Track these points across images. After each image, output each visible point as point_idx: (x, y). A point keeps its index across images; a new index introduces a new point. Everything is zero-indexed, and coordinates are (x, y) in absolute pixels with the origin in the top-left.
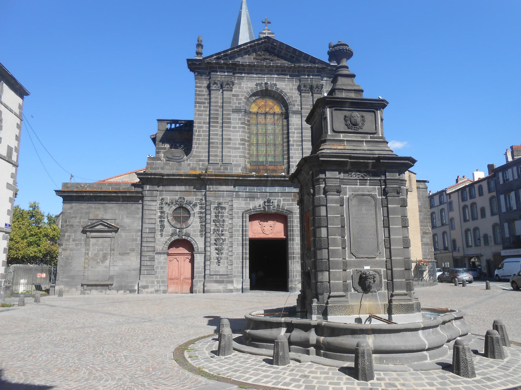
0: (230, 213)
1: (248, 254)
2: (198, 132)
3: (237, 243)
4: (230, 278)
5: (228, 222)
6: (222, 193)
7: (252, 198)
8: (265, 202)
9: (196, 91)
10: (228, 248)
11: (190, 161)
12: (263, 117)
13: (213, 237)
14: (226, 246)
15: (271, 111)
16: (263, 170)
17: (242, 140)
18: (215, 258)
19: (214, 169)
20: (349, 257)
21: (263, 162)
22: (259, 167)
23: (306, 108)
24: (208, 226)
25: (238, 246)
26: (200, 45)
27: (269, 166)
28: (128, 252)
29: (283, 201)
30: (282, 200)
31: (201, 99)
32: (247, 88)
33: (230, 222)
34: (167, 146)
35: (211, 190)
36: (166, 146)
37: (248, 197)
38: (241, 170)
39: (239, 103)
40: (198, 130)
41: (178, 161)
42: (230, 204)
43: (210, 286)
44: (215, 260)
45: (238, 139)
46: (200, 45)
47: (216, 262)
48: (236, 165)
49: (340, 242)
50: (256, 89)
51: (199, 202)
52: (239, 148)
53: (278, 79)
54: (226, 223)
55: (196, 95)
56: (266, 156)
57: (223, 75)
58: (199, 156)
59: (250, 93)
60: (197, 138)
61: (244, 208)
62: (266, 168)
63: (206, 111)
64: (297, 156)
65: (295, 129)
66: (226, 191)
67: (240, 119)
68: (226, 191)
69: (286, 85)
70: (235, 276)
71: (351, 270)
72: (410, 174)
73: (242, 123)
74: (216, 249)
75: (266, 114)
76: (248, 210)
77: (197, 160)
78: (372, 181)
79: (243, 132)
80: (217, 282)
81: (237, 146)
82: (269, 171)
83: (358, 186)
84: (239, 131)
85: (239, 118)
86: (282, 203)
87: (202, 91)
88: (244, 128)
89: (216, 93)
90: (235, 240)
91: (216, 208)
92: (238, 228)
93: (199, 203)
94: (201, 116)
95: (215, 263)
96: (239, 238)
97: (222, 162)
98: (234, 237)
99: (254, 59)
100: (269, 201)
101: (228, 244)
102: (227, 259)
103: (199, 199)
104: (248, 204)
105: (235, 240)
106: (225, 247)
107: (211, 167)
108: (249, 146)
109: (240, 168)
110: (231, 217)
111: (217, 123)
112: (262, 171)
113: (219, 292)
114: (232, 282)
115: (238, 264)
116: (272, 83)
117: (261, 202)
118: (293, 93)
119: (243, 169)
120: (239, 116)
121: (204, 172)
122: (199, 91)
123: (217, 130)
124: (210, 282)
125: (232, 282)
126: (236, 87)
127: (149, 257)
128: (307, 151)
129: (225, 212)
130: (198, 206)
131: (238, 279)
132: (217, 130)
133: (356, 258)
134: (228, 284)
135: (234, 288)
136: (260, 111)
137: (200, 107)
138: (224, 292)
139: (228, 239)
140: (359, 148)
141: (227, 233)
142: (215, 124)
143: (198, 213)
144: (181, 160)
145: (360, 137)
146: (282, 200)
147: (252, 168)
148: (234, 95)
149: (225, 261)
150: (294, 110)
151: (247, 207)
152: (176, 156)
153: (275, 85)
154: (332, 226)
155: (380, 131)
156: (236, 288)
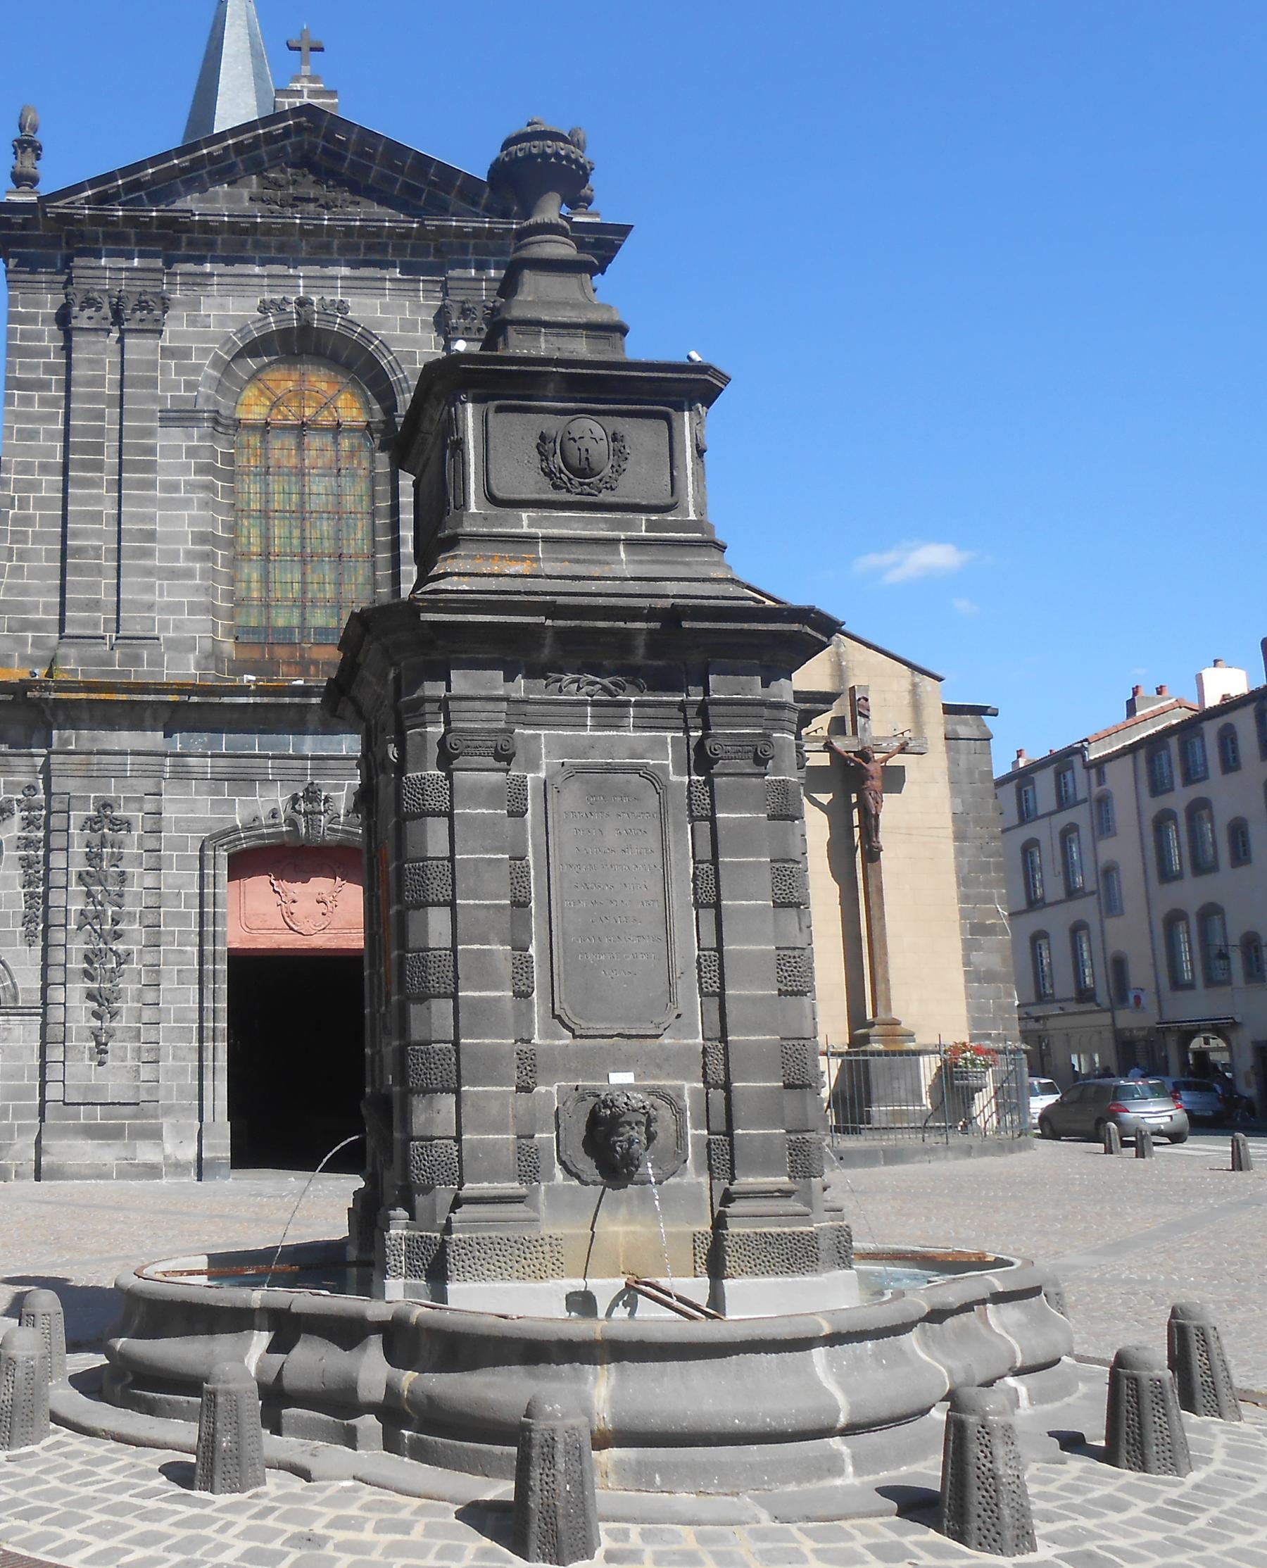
0: (151, 843)
1: (224, 1016)
3: (179, 971)
4: (146, 1117)
5: (139, 881)
6: (118, 759)
7: (243, 781)
8: (295, 799)
9: (11, 334)
10: (140, 991)
12: (290, 441)
13: (78, 946)
14: (132, 982)
15: (326, 419)
16: (289, 664)
17: (201, 538)
18: (87, 1033)
19: (82, 661)
20: (546, 1034)
21: (289, 630)
24: (56, 898)
26: (27, 145)
27: (315, 649)
31: (34, 368)
32: (222, 321)
33: (149, 881)
35: (72, 747)
37: (223, 776)
38: (198, 667)
39: (190, 386)
42: (149, 807)
43: (61, 1150)
44: (87, 1041)
45: (186, 533)
46: (27, 145)
47: (90, 1048)
49: (506, 969)
51: (21, 796)
52: (189, 574)
54: (133, 888)
55: (12, 350)
56: (303, 604)
57: (121, 269)
58: (22, 608)
61: (209, 824)
62: (302, 656)
63: (51, 418)
66: (133, 753)
68: (133, 753)
70: (168, 1110)
71: (554, 1089)
73: (201, 470)
74: (90, 996)
75: (302, 429)
76: (225, 834)
77: (15, 625)
78: (649, 711)
79: (205, 505)
80: (92, 1132)
81: (182, 564)
83: (589, 733)
84: (191, 499)
85: (188, 448)
87: (38, 336)
88: (209, 488)
89: (94, 343)
90: (172, 957)
91: (91, 824)
92: (182, 909)
93: (19, 801)
94: (31, 439)
95: (87, 1055)
96: (188, 948)
97: (118, 632)
98: (166, 944)
100: (311, 794)
102: (138, 1037)
103: (19, 783)
104: (224, 808)
105: (172, 957)
106: (128, 986)
107: (73, 652)
108: (233, 562)
109: (192, 658)
110: (152, 863)
111: (98, 466)
112: (283, 669)
113: (99, 1176)
114: (155, 1134)
115: (184, 1059)
117: (280, 799)
119: (203, 662)
120: (190, 437)
121: (40, 673)
122: (25, 335)
123: (98, 499)
124: (64, 1132)
125: (155, 1134)
126: (180, 318)
129: (127, 841)
130: (18, 815)
131: (182, 1121)
132: (98, 499)
133: (575, 1037)
134: (139, 1143)
135: (166, 1158)
136: (277, 418)
137: (27, 401)
138: (122, 1175)
139: (140, 952)
140: (596, 571)
141: (136, 926)
143: (15, 843)
145: (602, 526)
149: (126, 1047)
154: (472, 902)
155: (690, 499)
156: (173, 1160)
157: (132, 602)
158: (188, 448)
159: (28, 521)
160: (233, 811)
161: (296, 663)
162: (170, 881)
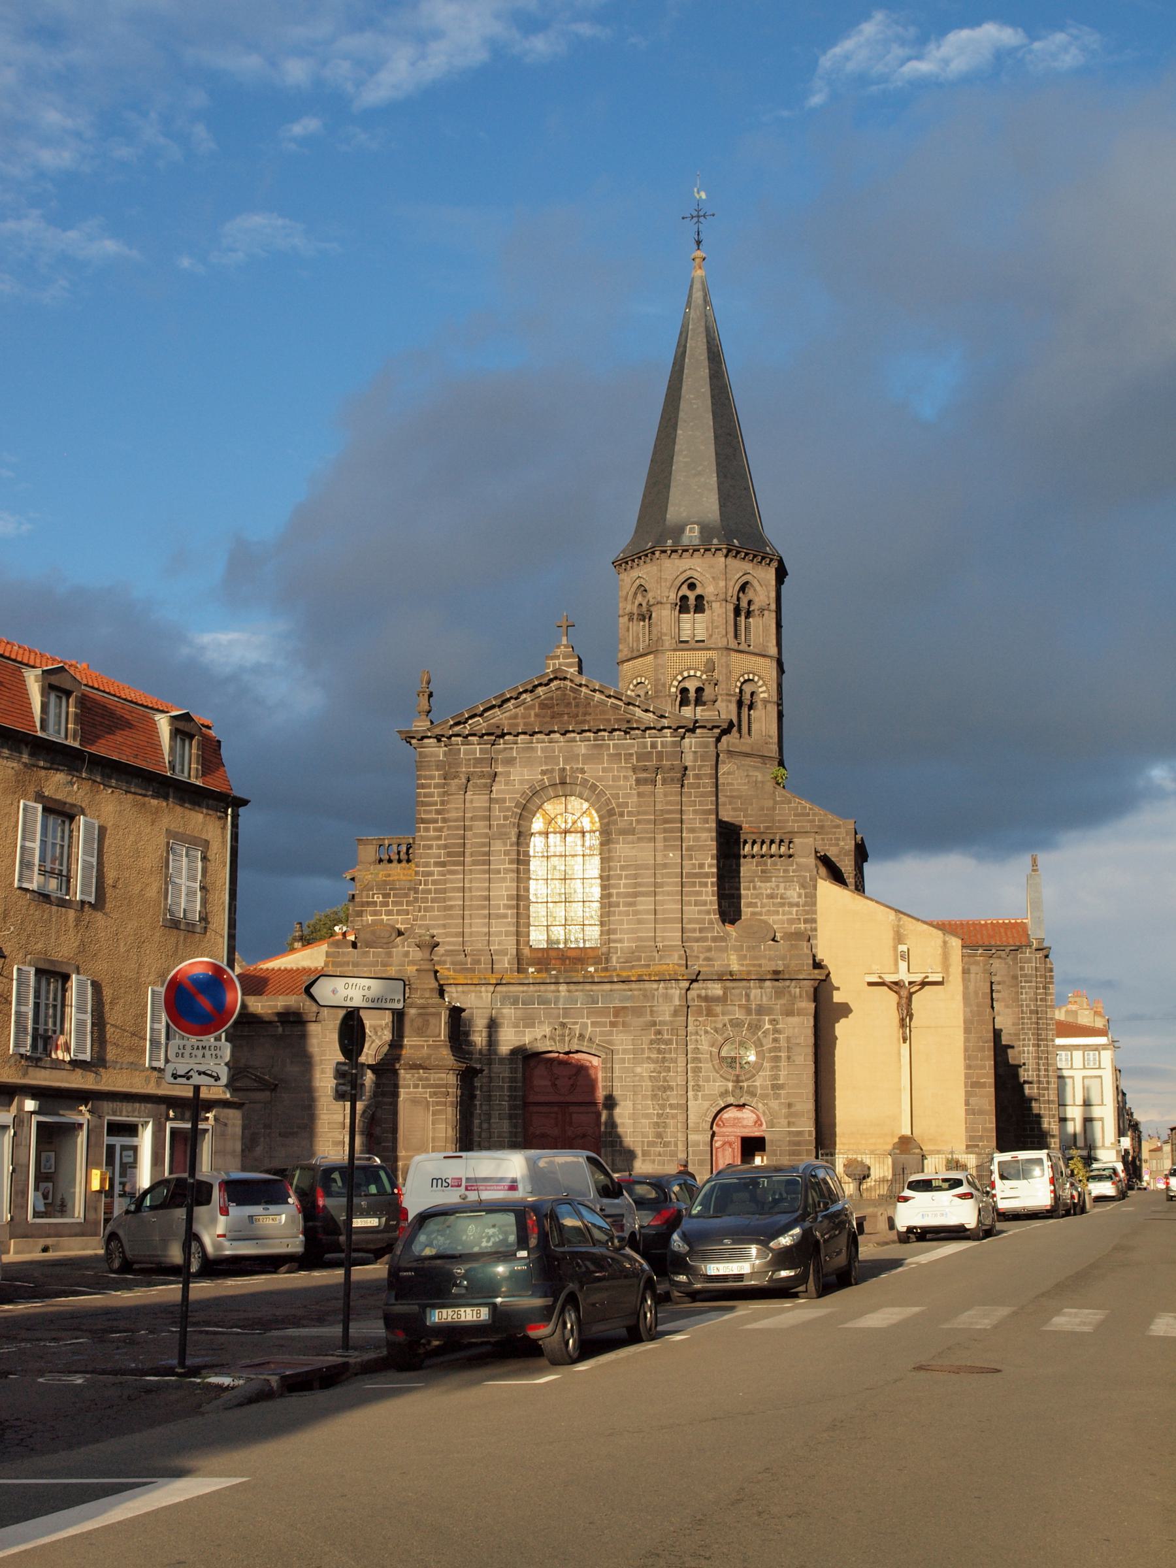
2: (425, 885)
3: (499, 1114)
11: (408, 947)
16: (556, 959)
17: (510, 898)
19: (453, 963)
22: (548, 954)
23: (645, 820)
25: (500, 1119)
28: (295, 1130)
29: (591, 1027)
30: (589, 1025)
31: (429, 812)
32: (522, 782)
34: (378, 898)
36: (375, 899)
38: (509, 964)
40: (425, 880)
41: (385, 946)
48: (498, 952)
50: (539, 783)
52: (505, 916)
53: (587, 758)
57: (470, 759)
59: (528, 794)
60: (421, 898)
62: (563, 955)
64: (625, 927)
65: (622, 868)
67: (507, 853)
69: (604, 770)
72: (947, 939)
73: (511, 862)
82: (567, 962)
85: (505, 850)
86: (590, 1029)
87: (431, 795)
90: (496, 1108)
99: (536, 715)
100: (563, 1025)
101: (480, 1115)
104: (521, 1035)
107: (448, 959)
109: (506, 959)
112: (553, 962)
116: (575, 767)
117: (547, 1030)
118: (619, 788)
127: (333, 1141)
128: (645, 917)
139: (481, 1104)
142: (456, 868)
144: (390, 945)
146: (589, 1025)
147: (533, 955)
148: (497, 801)
150: (621, 825)
151: (519, 1040)
152: (382, 935)
153: (583, 771)
157: (478, 932)
158: (505, 850)
159: (429, 891)
160: (524, 1035)
161: (560, 959)
162: (495, 1070)
